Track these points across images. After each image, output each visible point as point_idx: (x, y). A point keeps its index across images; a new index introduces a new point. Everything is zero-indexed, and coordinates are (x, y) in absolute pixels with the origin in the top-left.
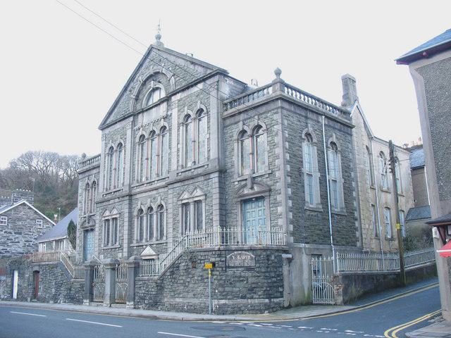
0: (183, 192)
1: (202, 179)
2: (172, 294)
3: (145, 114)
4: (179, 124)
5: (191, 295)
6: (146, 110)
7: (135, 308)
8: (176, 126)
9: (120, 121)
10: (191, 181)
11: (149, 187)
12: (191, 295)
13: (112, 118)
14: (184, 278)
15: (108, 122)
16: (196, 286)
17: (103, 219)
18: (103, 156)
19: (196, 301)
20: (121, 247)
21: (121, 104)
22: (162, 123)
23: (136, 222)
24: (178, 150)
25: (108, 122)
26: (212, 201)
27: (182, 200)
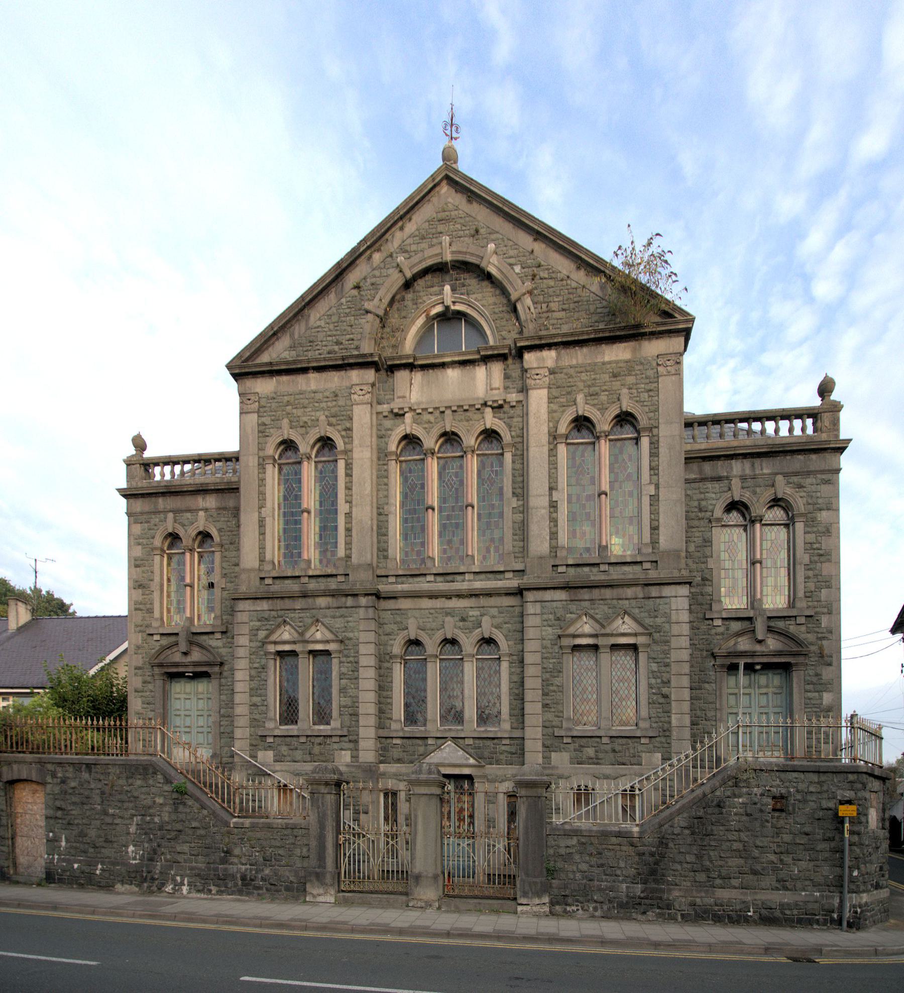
0: (580, 617)
1: (639, 591)
2: (702, 877)
3: (418, 376)
4: (554, 437)
5: (769, 880)
6: (424, 367)
7: (552, 914)
8: (545, 439)
9: (320, 369)
10: (608, 593)
11: (441, 586)
12: (769, 880)
13: (280, 352)
14: (743, 836)
15: (265, 358)
16: (788, 859)
17: (272, 648)
18: (250, 462)
19: (786, 897)
20: (351, 738)
21: (315, 315)
22: (490, 420)
23: (398, 673)
24: (553, 505)
25: (265, 358)
26: (667, 653)
27: (575, 636)
